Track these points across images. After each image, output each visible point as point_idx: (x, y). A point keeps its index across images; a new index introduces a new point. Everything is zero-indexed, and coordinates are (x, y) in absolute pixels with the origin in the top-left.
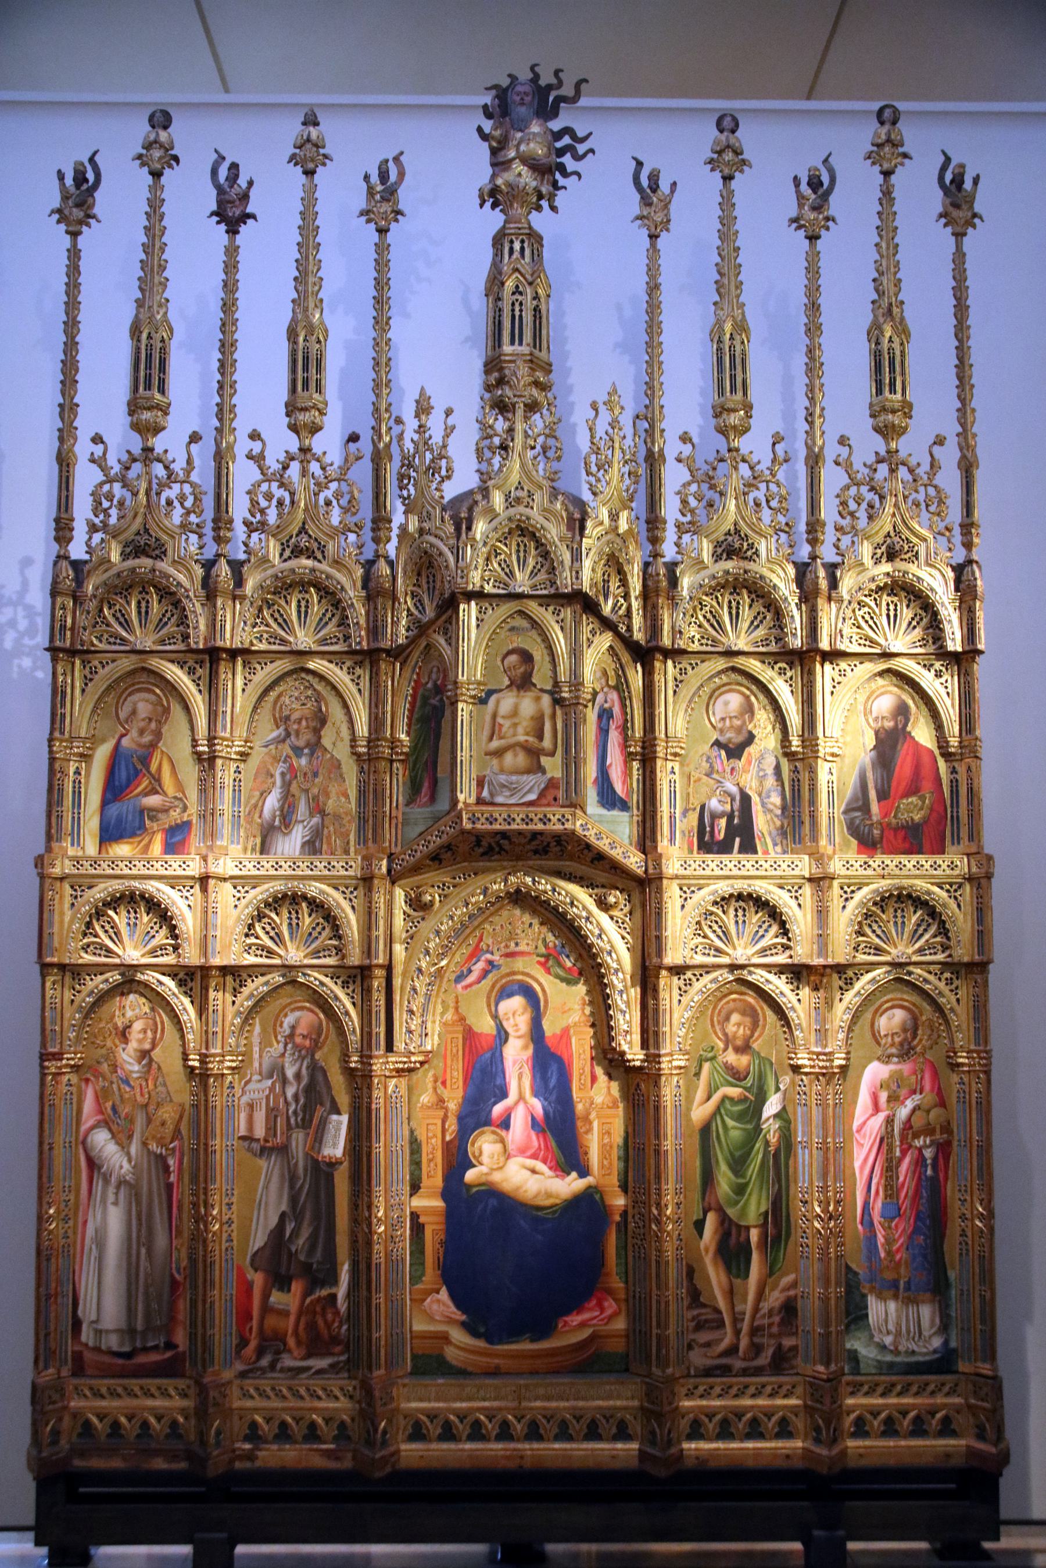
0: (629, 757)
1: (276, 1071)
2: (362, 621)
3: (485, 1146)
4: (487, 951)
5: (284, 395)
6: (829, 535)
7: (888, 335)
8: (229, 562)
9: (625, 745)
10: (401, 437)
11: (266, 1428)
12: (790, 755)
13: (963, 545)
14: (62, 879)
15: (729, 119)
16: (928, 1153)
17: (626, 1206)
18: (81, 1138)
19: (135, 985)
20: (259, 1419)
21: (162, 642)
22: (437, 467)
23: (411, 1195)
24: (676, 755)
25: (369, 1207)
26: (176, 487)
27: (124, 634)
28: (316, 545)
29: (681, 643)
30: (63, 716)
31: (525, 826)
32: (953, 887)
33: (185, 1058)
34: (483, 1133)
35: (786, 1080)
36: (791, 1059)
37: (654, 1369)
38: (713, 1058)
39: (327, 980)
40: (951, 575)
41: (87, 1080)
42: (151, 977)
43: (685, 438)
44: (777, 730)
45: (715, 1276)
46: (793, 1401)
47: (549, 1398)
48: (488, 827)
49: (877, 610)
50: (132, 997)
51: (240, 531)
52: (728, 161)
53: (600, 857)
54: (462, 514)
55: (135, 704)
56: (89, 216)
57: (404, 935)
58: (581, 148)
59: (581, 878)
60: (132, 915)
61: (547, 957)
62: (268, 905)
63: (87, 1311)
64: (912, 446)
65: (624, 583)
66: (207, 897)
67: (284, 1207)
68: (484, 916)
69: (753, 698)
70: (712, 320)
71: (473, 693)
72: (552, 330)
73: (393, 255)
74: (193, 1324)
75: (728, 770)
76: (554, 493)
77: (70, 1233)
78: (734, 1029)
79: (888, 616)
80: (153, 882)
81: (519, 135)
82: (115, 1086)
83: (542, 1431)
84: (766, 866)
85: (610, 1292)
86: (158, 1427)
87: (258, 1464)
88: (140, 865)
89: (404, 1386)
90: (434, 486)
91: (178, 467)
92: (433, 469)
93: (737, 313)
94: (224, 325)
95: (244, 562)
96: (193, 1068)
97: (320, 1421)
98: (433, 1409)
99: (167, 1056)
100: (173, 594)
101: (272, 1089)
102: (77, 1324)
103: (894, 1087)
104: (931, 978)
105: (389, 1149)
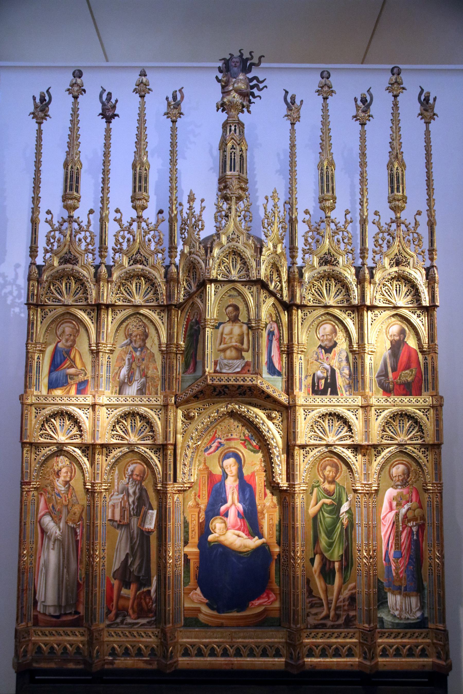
0: (281, 352)
1: (125, 491)
2: (164, 292)
3: (217, 524)
4: (218, 438)
5: (130, 193)
6: (370, 255)
7: (396, 167)
8: (106, 266)
9: (280, 347)
10: (181, 211)
11: (119, 650)
12: (353, 352)
13: (430, 259)
14: (31, 405)
15: (326, 73)
16: (414, 529)
17: (279, 552)
18: (38, 520)
19: (63, 452)
20: (116, 646)
21: (76, 301)
22: (197, 224)
23: (184, 546)
24: (302, 351)
25: (166, 551)
26: (83, 233)
27: (60, 297)
28: (144, 259)
29: (305, 302)
30: (33, 333)
31: (235, 383)
32: (425, 410)
33: (85, 485)
34: (216, 519)
35: (351, 496)
37: (292, 625)
38: (319, 486)
39: (148, 451)
40: (424, 272)
41: (41, 494)
42: (70, 449)
43: (307, 212)
44: (347, 341)
45: (319, 583)
46: (354, 640)
47: (244, 638)
48: (219, 383)
49: (391, 288)
50: (61, 457)
51: (111, 252)
52: (326, 91)
53: (268, 397)
54: (208, 245)
55: (64, 328)
56: (46, 116)
57: (182, 431)
58: (261, 86)
59: (260, 406)
60: (62, 421)
61: (245, 441)
62: (122, 417)
63: (40, 597)
64: (407, 215)
65: (279, 276)
66: (95, 413)
67: (128, 551)
68: (217, 422)
69: (336, 327)
70: (318, 160)
71: (213, 324)
72: (248, 165)
73: (178, 132)
74: (87, 602)
75: (325, 358)
76: (249, 236)
77: (33, 562)
78: (328, 473)
79: (396, 290)
80: (71, 407)
81: (234, 80)
82: (53, 497)
83: (242, 653)
84: (342, 400)
85: (272, 590)
86: (71, 649)
87: (115, 666)
88: (65, 399)
89: (181, 631)
90: (196, 233)
91: (84, 224)
92: (195, 226)
93: (330, 157)
94: (104, 162)
95: (112, 266)
96: (88, 489)
97: (143, 647)
98: (194, 642)
99: (77, 484)
100: (81, 280)
101: (123, 498)
102: (35, 603)
103: (399, 499)
105: (174, 525)
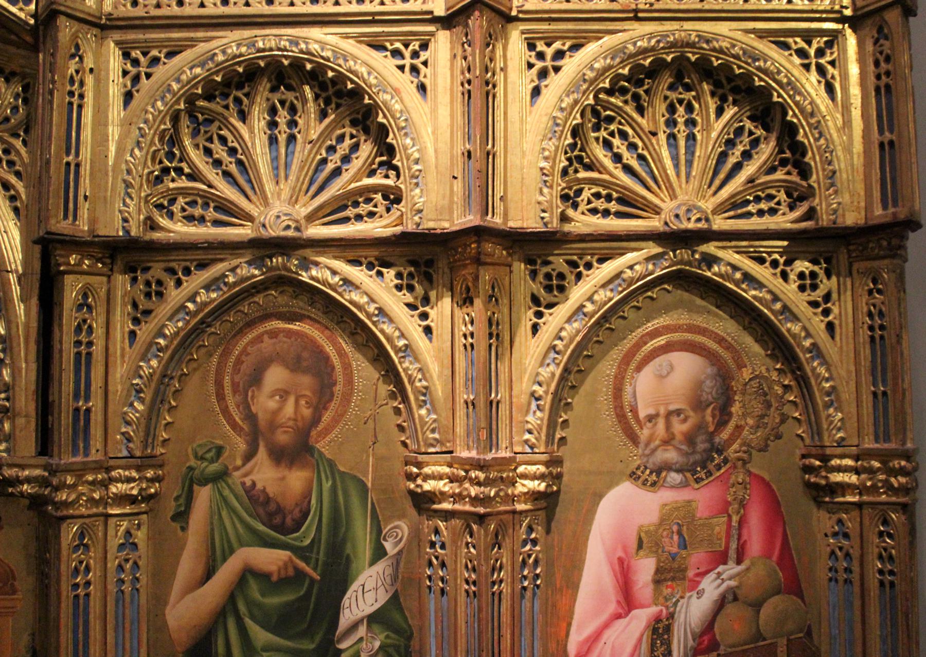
35: (399, 531)
36: (411, 477)
78: (272, 404)
103: (672, 545)
104: (762, 272)
